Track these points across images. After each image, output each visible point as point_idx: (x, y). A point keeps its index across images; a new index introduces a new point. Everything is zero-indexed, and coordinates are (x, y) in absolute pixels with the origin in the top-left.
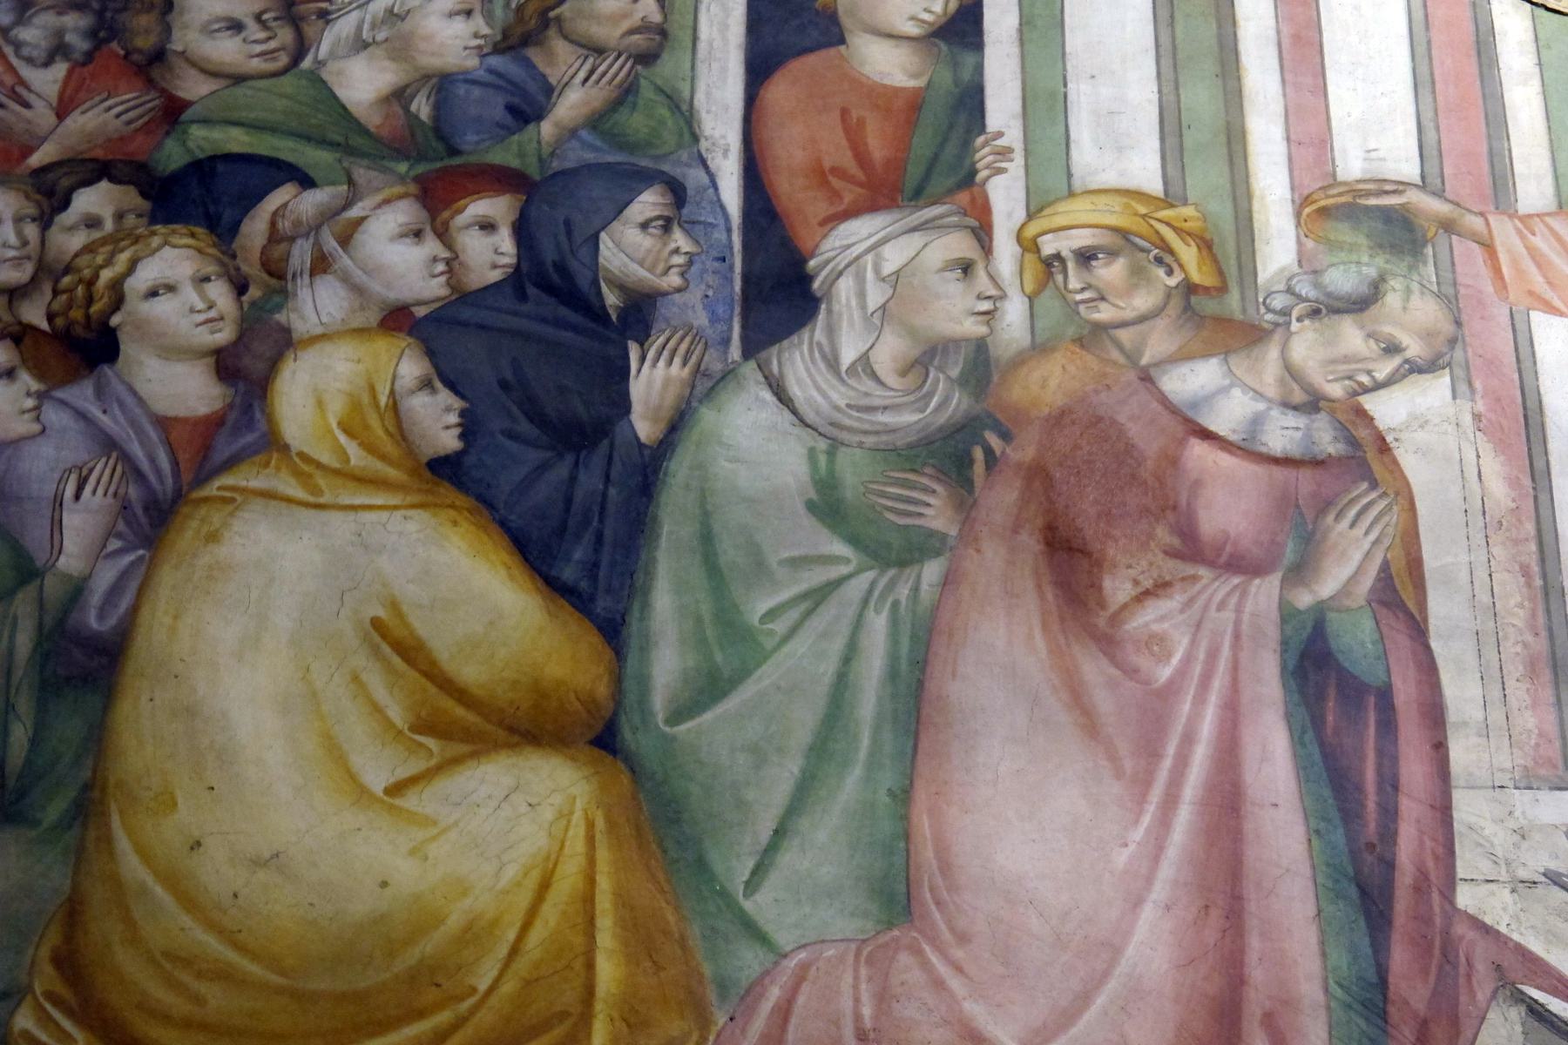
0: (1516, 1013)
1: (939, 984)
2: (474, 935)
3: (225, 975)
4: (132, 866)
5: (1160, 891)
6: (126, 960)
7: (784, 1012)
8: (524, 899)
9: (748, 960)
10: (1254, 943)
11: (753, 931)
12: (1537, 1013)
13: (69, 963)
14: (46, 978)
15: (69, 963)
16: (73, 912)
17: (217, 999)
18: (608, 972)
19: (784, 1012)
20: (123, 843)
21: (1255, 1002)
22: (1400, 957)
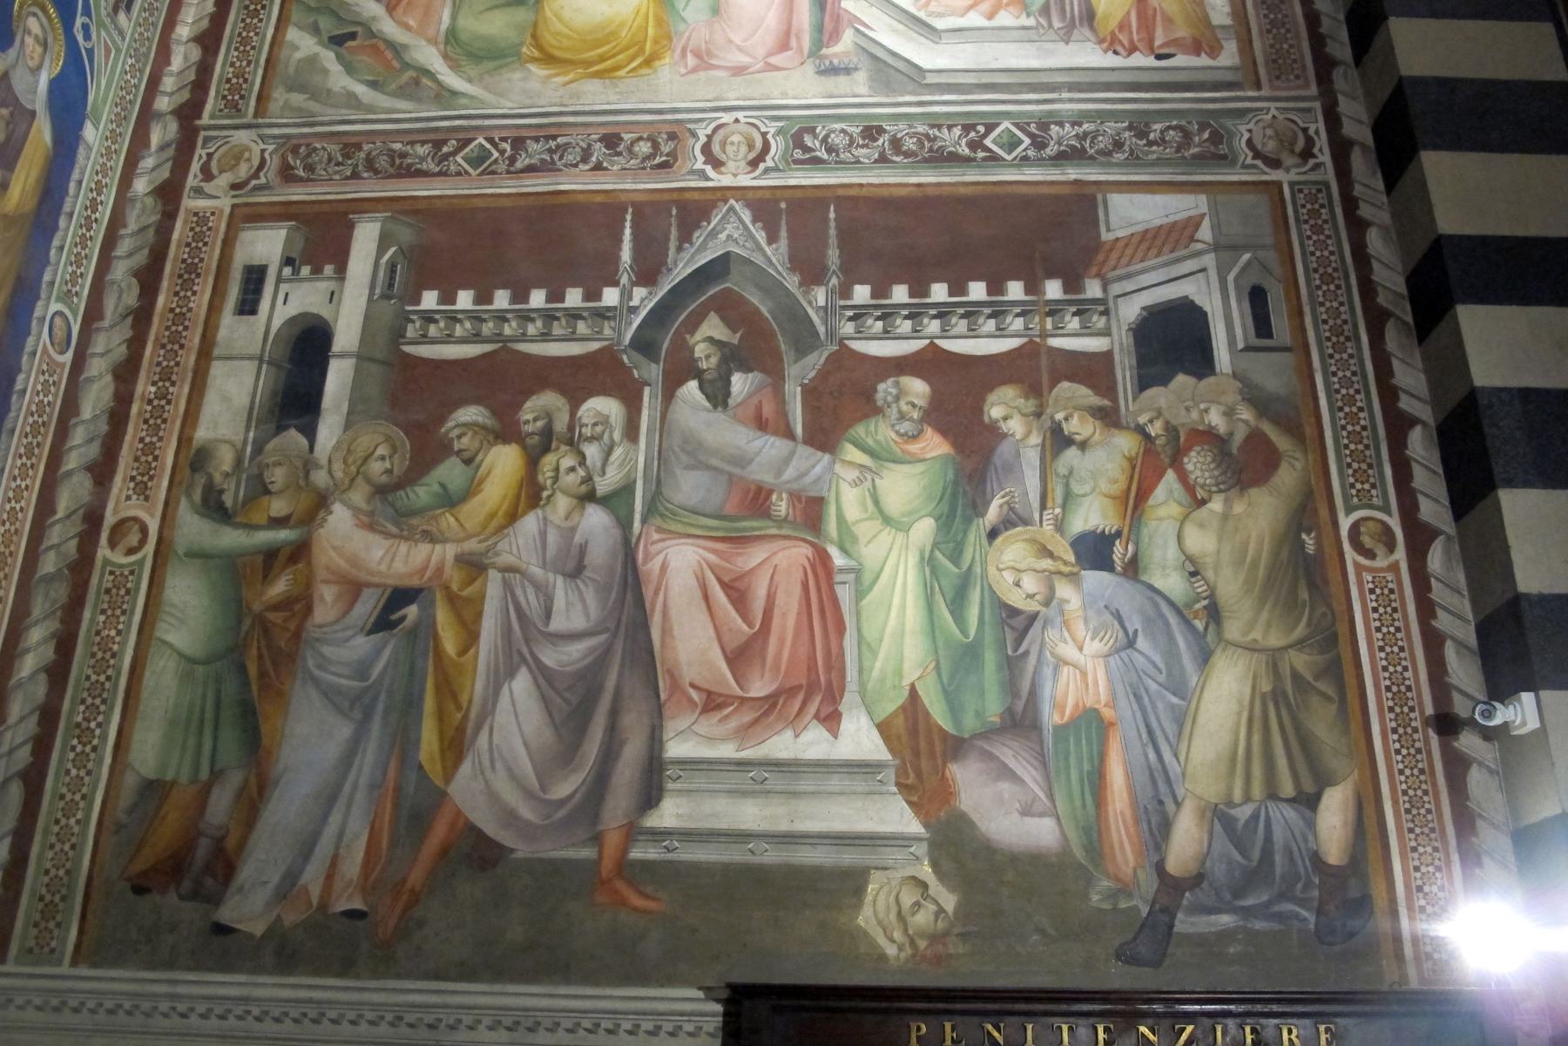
0: (852, 30)
1: (723, 30)
2: (622, 25)
3: (569, 37)
4: (548, 13)
5: (775, 6)
6: (546, 34)
7: (689, 38)
8: (633, 16)
9: (682, 27)
10: (795, 17)
11: (683, 20)
12: (857, 30)
13: (534, 36)
14: (529, 39)
15: (534, 36)
16: (535, 25)
17: (566, 43)
18: (651, 31)
19: (689, 38)
20: (547, 9)
21: (793, 31)
22: (827, 18)
